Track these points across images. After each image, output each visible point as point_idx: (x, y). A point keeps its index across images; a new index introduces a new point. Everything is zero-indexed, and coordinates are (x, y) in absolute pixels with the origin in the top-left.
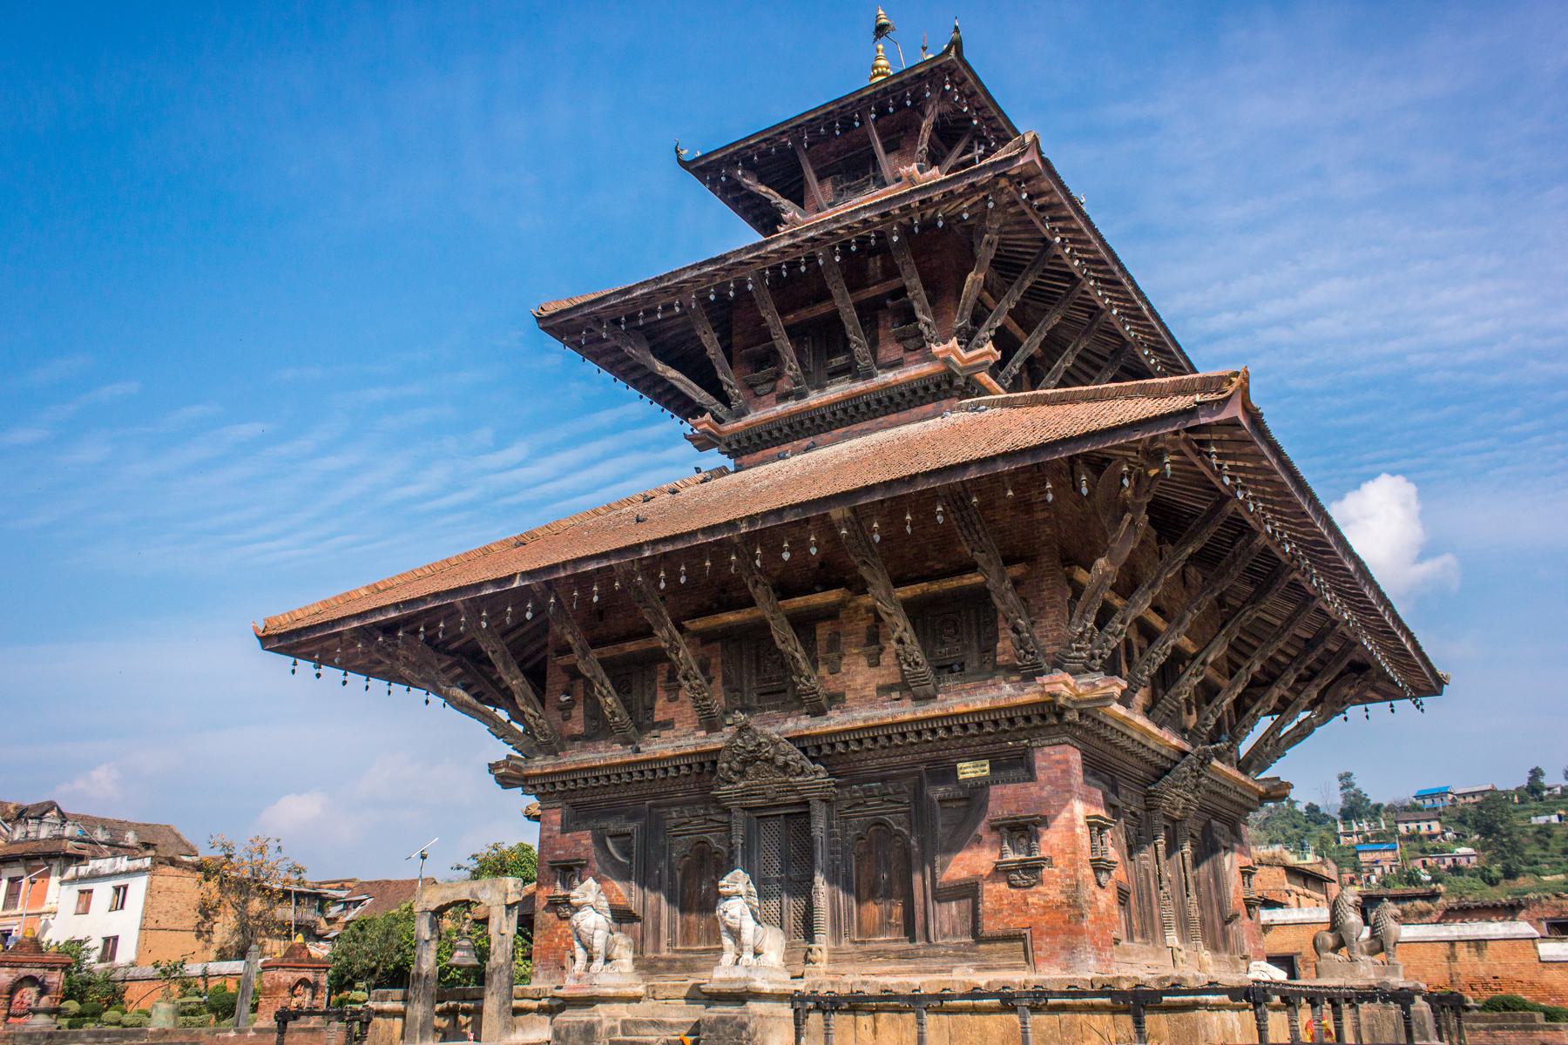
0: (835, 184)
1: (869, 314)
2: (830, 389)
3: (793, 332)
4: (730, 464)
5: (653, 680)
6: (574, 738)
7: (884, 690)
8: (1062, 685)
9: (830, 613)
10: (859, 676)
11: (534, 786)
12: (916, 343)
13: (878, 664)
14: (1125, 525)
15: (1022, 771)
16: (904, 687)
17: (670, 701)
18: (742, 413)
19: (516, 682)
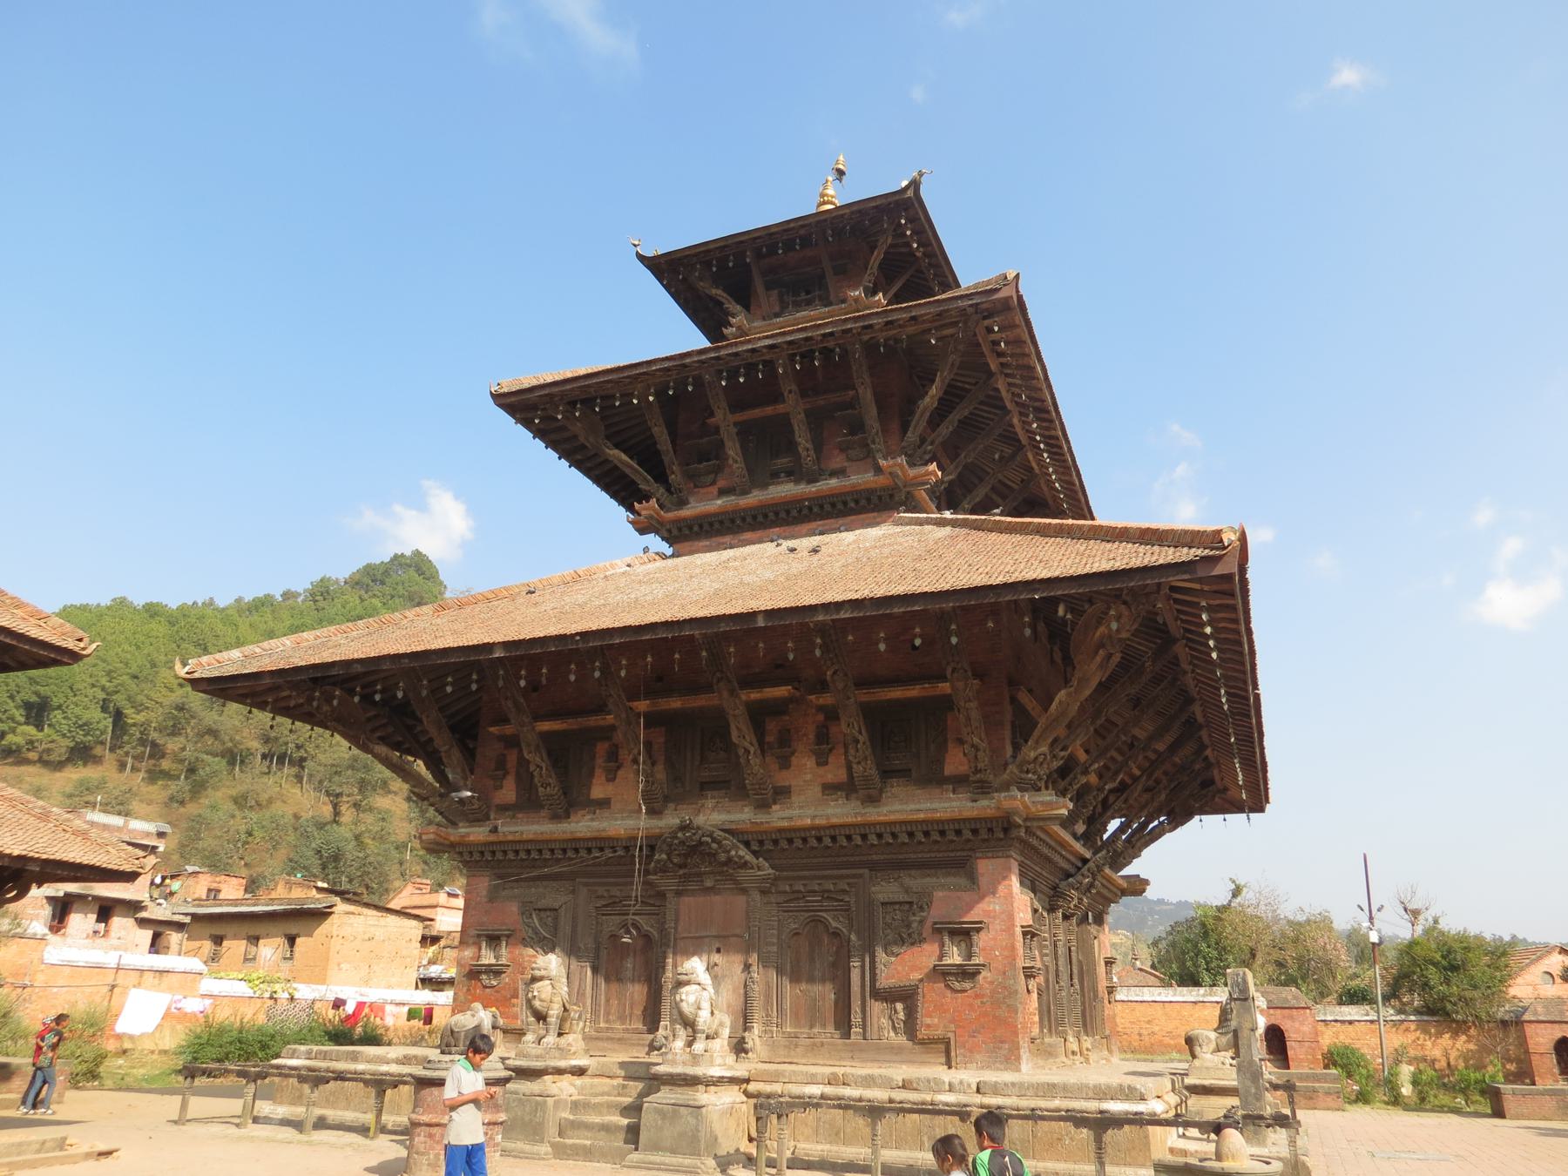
0: (781, 296)
1: (816, 420)
3: (744, 431)
4: (669, 551)
5: (593, 758)
6: (504, 808)
7: (830, 789)
8: (1020, 802)
9: (777, 709)
10: (806, 774)
11: (461, 853)
12: (867, 456)
13: (826, 763)
14: (1098, 659)
15: (963, 881)
16: (847, 788)
17: (608, 780)
18: (682, 503)
19: (443, 742)
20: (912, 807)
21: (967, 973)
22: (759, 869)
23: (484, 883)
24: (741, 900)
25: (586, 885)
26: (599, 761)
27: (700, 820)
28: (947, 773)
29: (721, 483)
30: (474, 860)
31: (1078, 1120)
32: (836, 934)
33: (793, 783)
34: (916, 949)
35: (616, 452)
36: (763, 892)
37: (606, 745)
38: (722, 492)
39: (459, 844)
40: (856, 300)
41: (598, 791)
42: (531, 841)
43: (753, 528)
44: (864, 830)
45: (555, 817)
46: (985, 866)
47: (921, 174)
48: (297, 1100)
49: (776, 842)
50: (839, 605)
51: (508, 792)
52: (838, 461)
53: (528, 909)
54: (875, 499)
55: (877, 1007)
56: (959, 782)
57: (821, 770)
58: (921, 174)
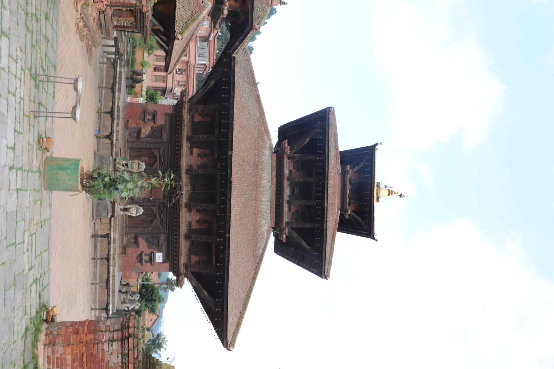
2: (289, 187)
6: (193, 117)
7: (190, 223)
20: (183, 248)
21: (141, 261)
23: (170, 111)
24: (162, 197)
26: (204, 151)
27: (184, 192)
28: (192, 256)
29: (293, 171)
30: (179, 107)
31: (108, 305)
32: (152, 222)
33: (192, 213)
34: (147, 247)
35: (308, 140)
36: (163, 203)
38: (290, 171)
39: (183, 105)
40: (347, 211)
42: (181, 131)
43: (277, 182)
44: (178, 235)
46: (167, 265)
47: (377, 241)
48: (107, 82)
50: (229, 257)
51: (197, 119)
52: (293, 209)
53: (161, 128)
54: (278, 222)
55: (133, 235)
56: (189, 259)
57: (195, 221)
58: (377, 241)
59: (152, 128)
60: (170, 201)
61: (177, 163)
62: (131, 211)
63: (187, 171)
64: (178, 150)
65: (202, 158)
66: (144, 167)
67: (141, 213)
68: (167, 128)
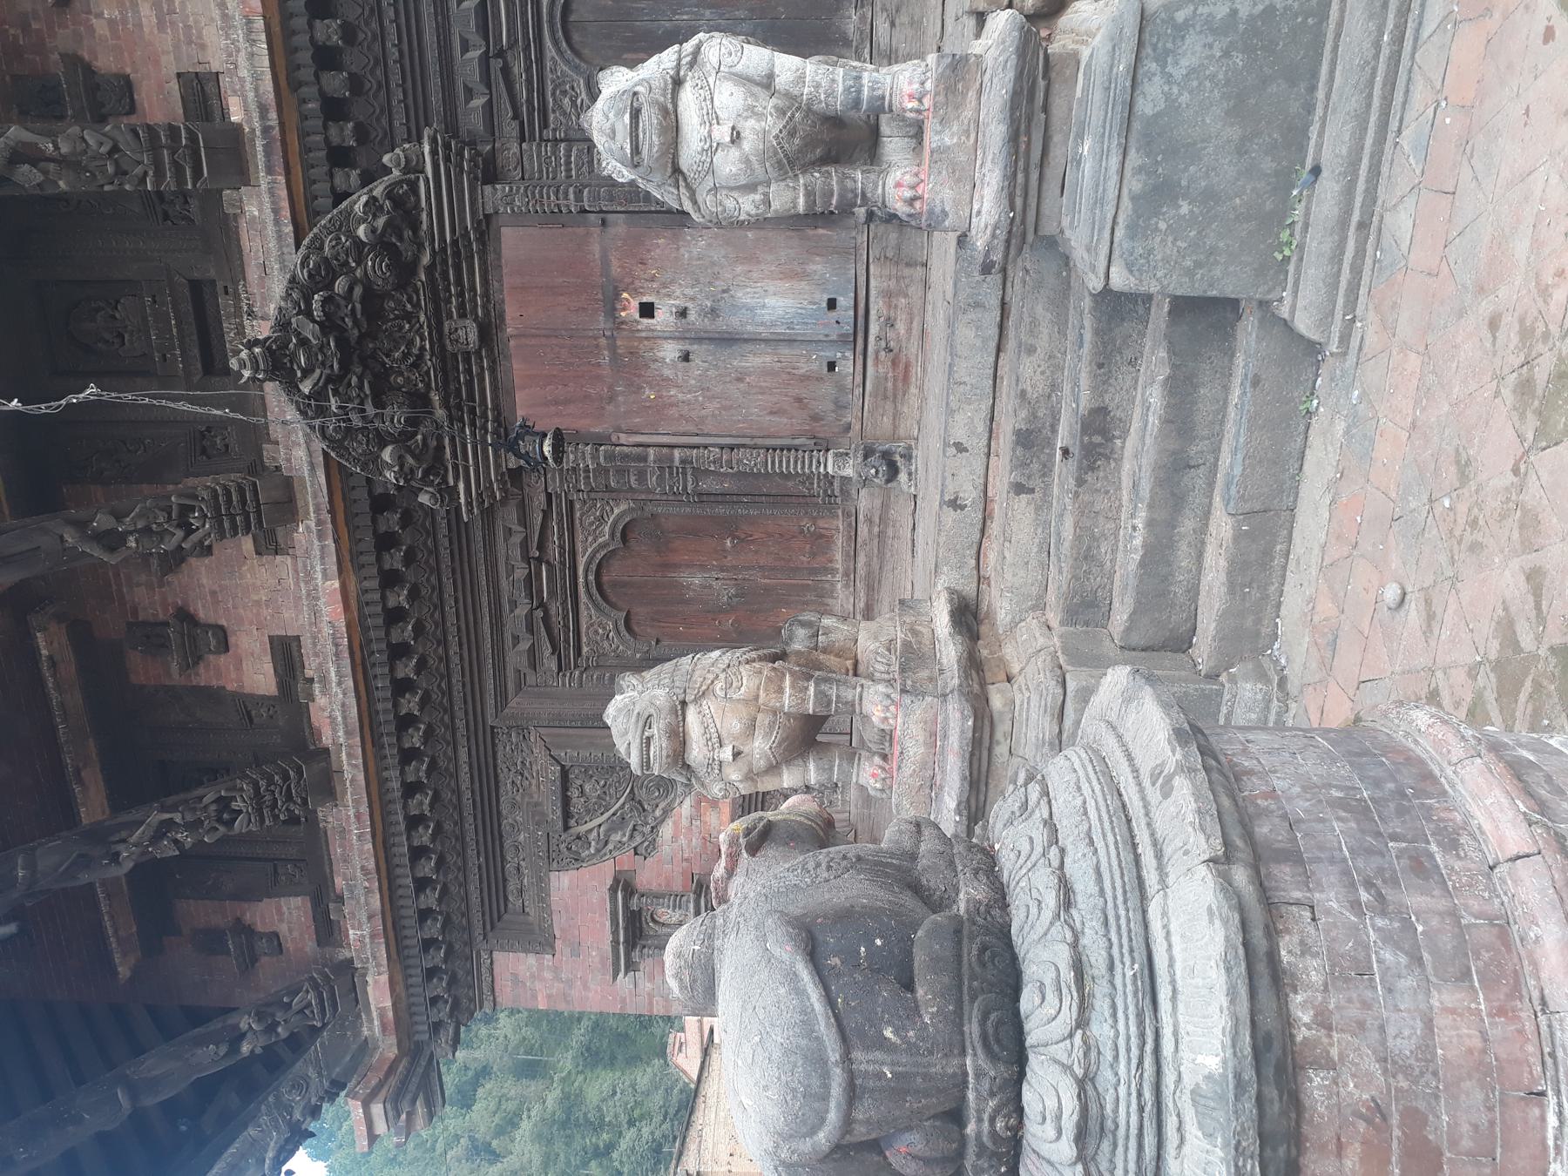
6: (327, 929)
11: (437, 1027)
17: (224, 646)
22: (413, 168)
24: (513, 242)
25: (502, 698)
26: (176, 677)
33: (169, 66)
36: (491, 173)
37: (135, 658)
41: (260, 678)
45: (327, 787)
49: (334, 109)
51: (287, 916)
53: (567, 850)
59: (645, 849)
60: (403, 206)
61: (390, 580)
62: (762, 128)
63: (287, 506)
64: (402, 687)
65: (185, 617)
66: (613, 713)
67: (616, 81)
68: (521, 834)
